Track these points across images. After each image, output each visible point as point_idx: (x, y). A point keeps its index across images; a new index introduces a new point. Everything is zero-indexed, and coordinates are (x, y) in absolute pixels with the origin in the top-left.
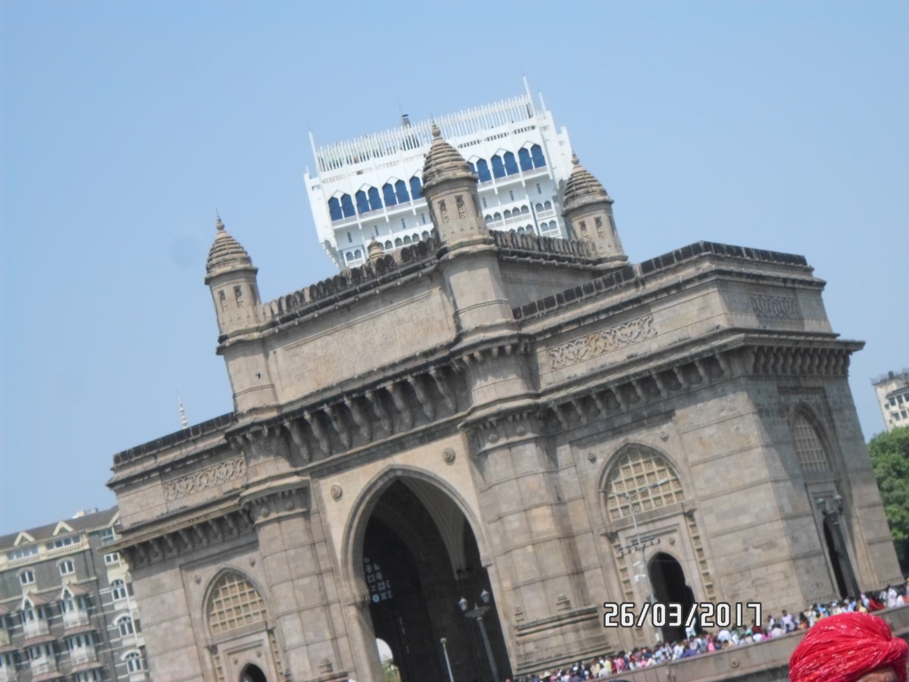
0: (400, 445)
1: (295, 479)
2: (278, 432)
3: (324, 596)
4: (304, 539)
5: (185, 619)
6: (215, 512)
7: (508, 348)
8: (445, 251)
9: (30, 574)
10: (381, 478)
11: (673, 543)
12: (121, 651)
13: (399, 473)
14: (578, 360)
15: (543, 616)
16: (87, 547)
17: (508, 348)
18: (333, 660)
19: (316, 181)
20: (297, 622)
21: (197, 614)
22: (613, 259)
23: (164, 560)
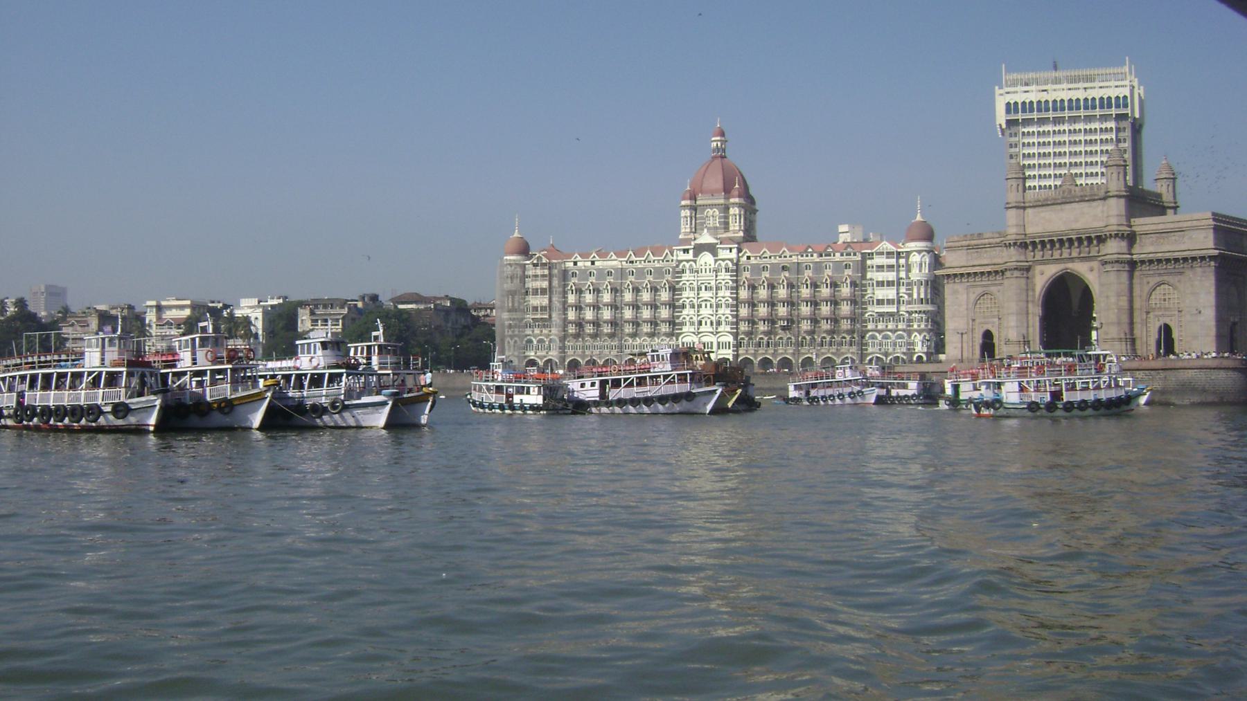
0: (1071, 259)
1: (1026, 264)
2: (1023, 245)
3: (1027, 311)
4: (1024, 287)
5: (965, 307)
6: (988, 269)
7: (1125, 235)
8: (1109, 192)
9: (830, 266)
10: (1061, 271)
11: (1171, 320)
12: (866, 313)
13: (1069, 271)
14: (1152, 244)
15: (1115, 336)
16: (860, 259)
17: (1125, 235)
18: (1026, 335)
19: (1002, 91)
20: (1015, 318)
21: (970, 306)
22: (1171, 203)
23: (961, 282)
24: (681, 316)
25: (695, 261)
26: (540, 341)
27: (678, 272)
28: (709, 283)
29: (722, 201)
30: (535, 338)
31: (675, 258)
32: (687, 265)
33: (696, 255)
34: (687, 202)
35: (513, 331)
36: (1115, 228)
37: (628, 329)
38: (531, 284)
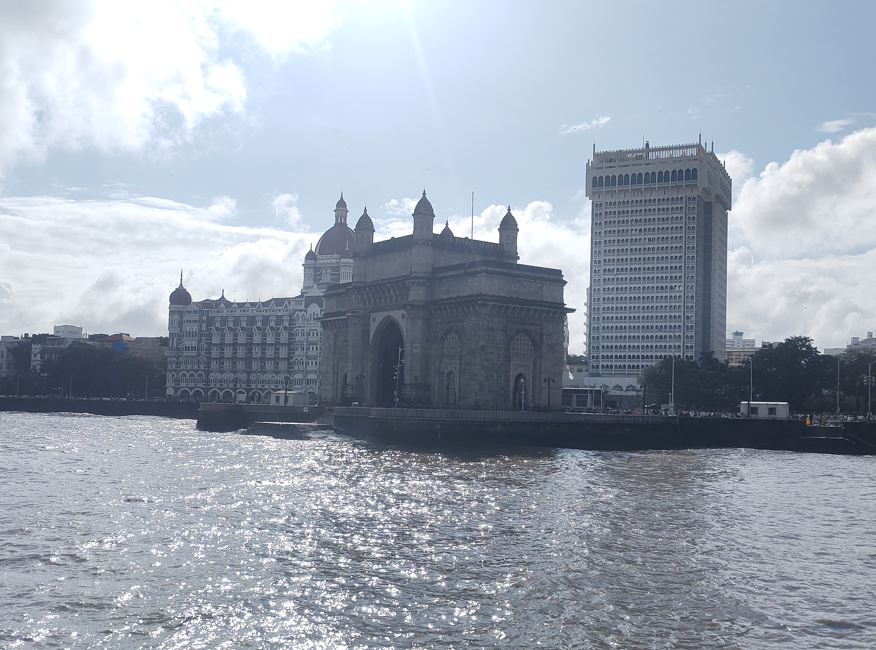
7: (422, 283)
17: (422, 283)
24: (294, 356)
25: (306, 311)
26: (192, 375)
27: (294, 320)
28: (316, 330)
29: (334, 261)
30: (188, 371)
31: (291, 308)
32: (300, 314)
33: (307, 306)
34: (309, 262)
35: (171, 367)
36: (414, 275)
37: (255, 366)
38: (187, 328)
